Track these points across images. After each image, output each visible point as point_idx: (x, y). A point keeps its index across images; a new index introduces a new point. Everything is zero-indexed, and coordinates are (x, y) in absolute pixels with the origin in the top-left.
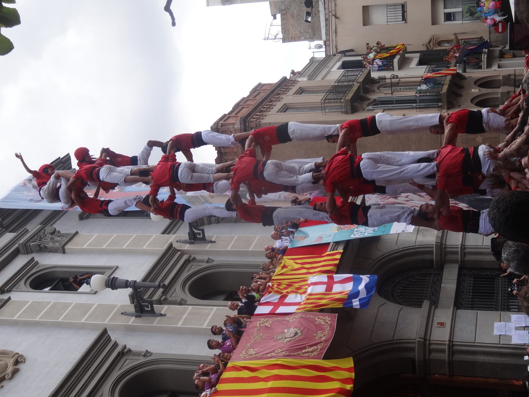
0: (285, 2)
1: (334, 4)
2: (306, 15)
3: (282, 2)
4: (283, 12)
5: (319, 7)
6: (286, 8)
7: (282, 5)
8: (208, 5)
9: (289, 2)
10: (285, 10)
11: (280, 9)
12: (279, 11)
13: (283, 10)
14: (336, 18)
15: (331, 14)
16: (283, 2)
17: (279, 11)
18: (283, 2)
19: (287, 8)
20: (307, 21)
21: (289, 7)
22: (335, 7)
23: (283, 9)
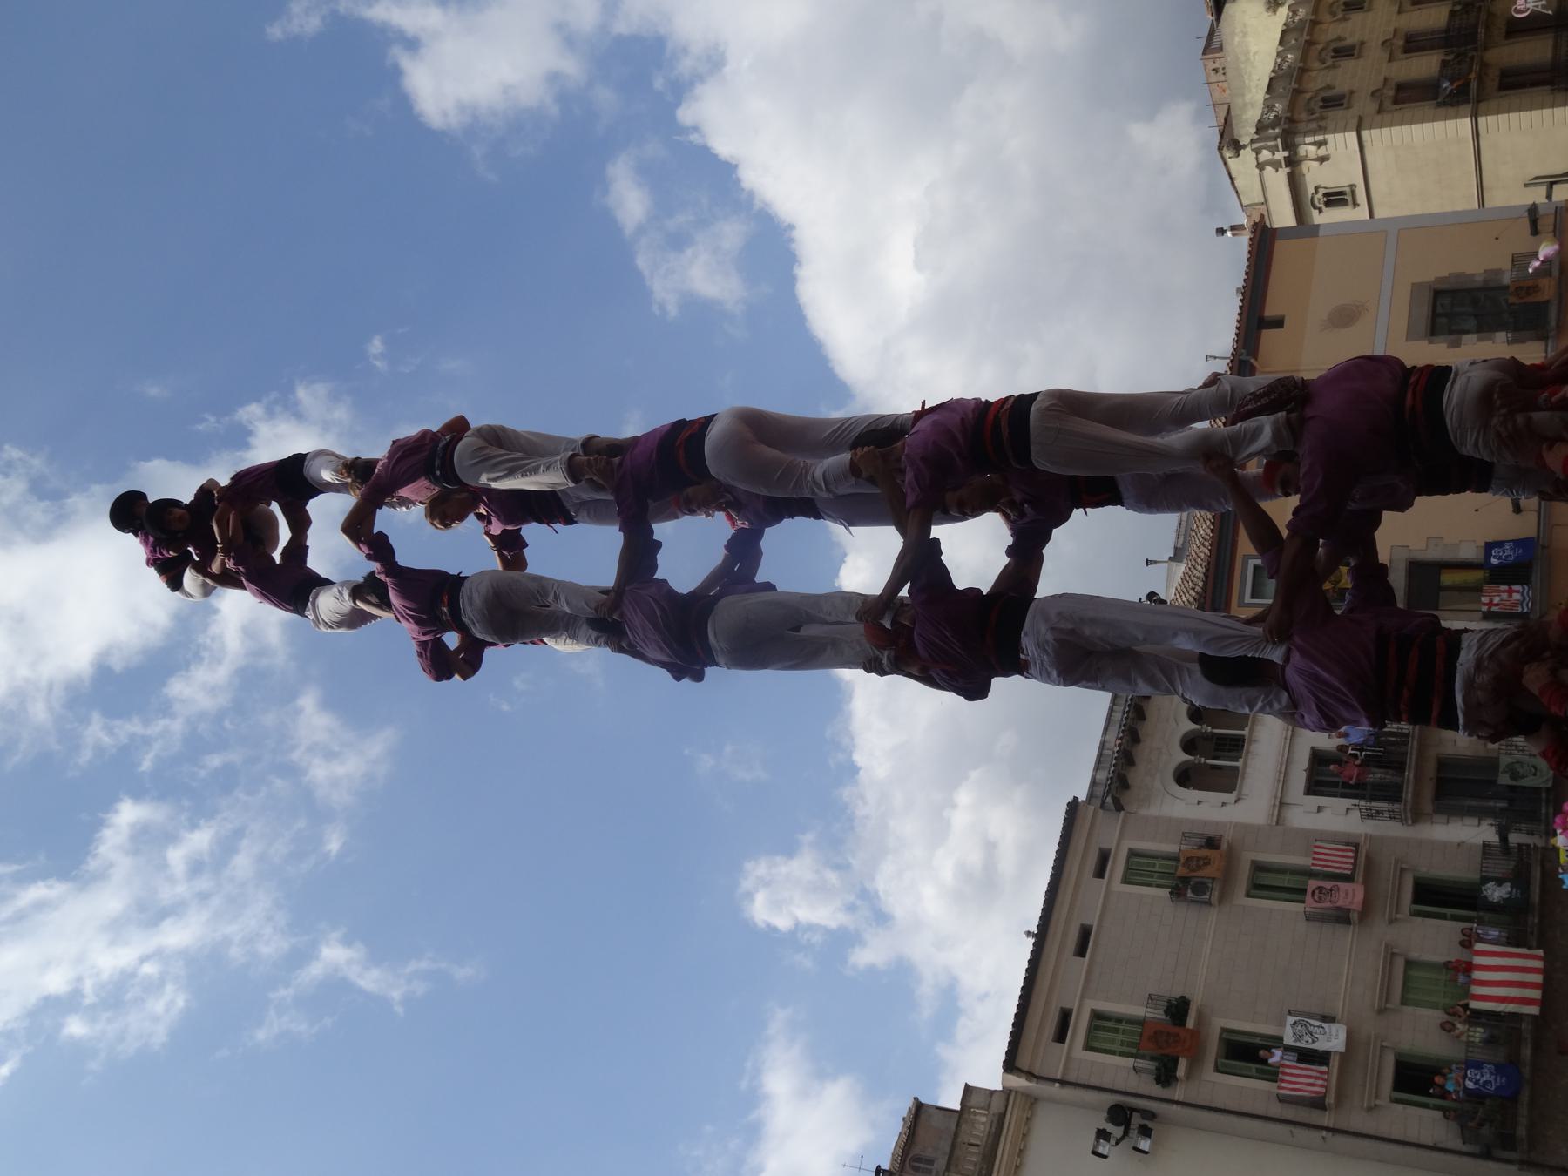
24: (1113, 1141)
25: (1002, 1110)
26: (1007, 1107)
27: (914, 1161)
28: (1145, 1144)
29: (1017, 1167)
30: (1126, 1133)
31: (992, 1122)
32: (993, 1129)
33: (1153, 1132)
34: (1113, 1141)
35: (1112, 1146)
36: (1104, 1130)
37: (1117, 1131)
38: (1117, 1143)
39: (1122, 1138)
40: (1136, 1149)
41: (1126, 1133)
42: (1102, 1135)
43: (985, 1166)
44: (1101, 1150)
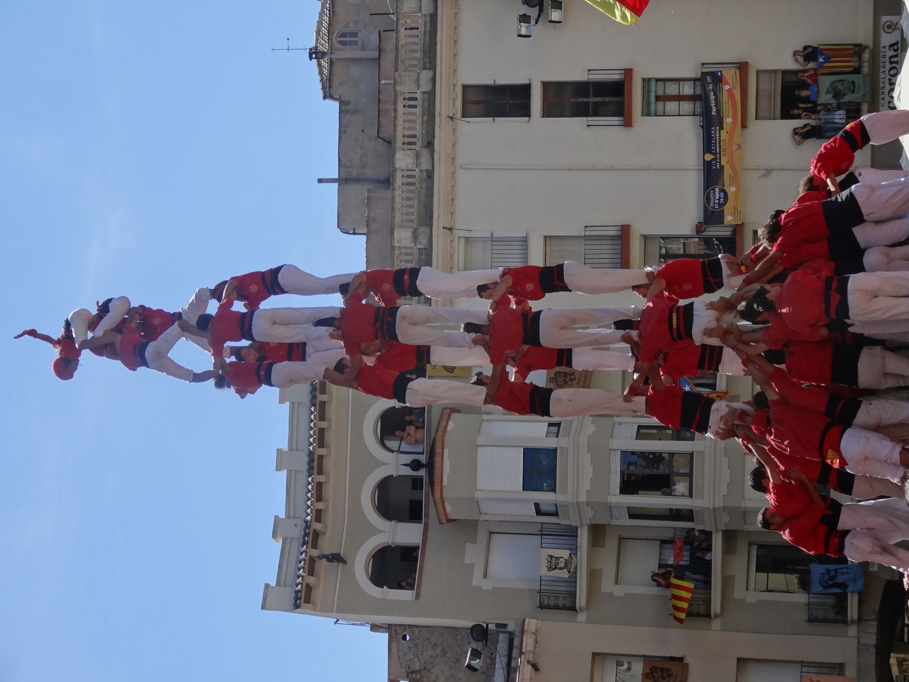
0: (422, 655)
1: (533, 639)
2: (471, 654)
3: (416, 653)
4: (414, 675)
5: (494, 675)
6: (423, 668)
7: (416, 660)
8: (263, 608)
9: (431, 657)
10: (419, 671)
11: (409, 668)
12: (406, 672)
13: (414, 672)
14: (535, 667)
15: (524, 659)
16: (420, 654)
17: (406, 674)
18: (420, 654)
19: (425, 668)
20: (469, 667)
21: (430, 667)
22: (535, 647)
23: (417, 668)
24: (533, 21)
25: (432, 11)
26: (436, 8)
27: (339, 37)
28: (555, 15)
29: (455, 55)
30: (541, 10)
31: (425, 22)
32: (428, 28)
33: (563, 4)
34: (533, 21)
35: (533, 25)
36: (525, 15)
37: (533, 12)
38: (536, 23)
39: (539, 16)
40: (551, 21)
41: (541, 10)
42: (524, 19)
43: (428, 60)
44: (523, 32)
